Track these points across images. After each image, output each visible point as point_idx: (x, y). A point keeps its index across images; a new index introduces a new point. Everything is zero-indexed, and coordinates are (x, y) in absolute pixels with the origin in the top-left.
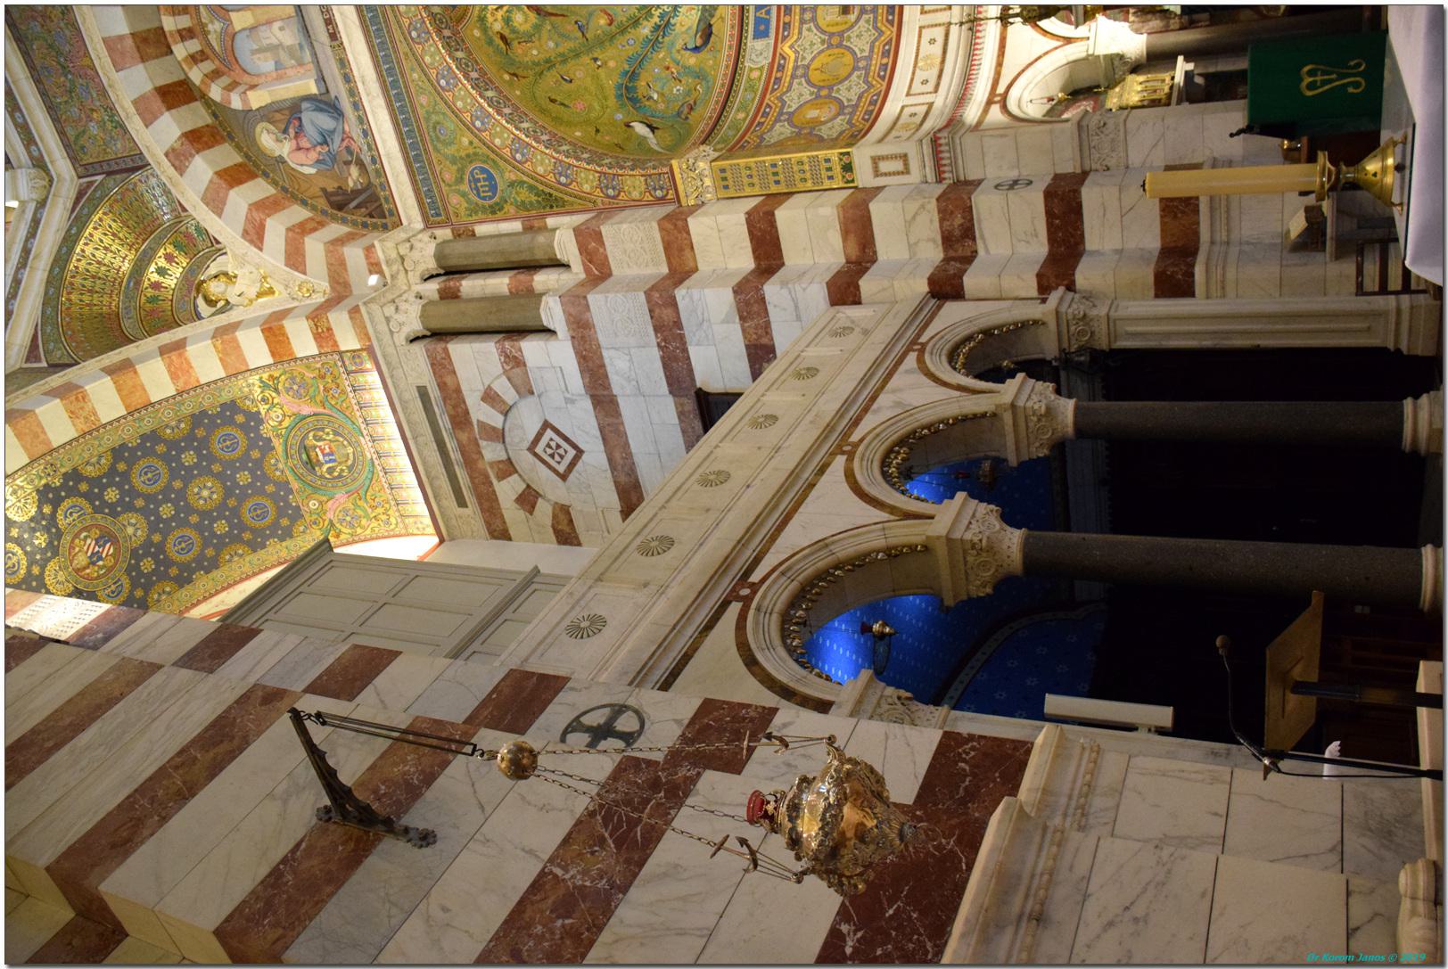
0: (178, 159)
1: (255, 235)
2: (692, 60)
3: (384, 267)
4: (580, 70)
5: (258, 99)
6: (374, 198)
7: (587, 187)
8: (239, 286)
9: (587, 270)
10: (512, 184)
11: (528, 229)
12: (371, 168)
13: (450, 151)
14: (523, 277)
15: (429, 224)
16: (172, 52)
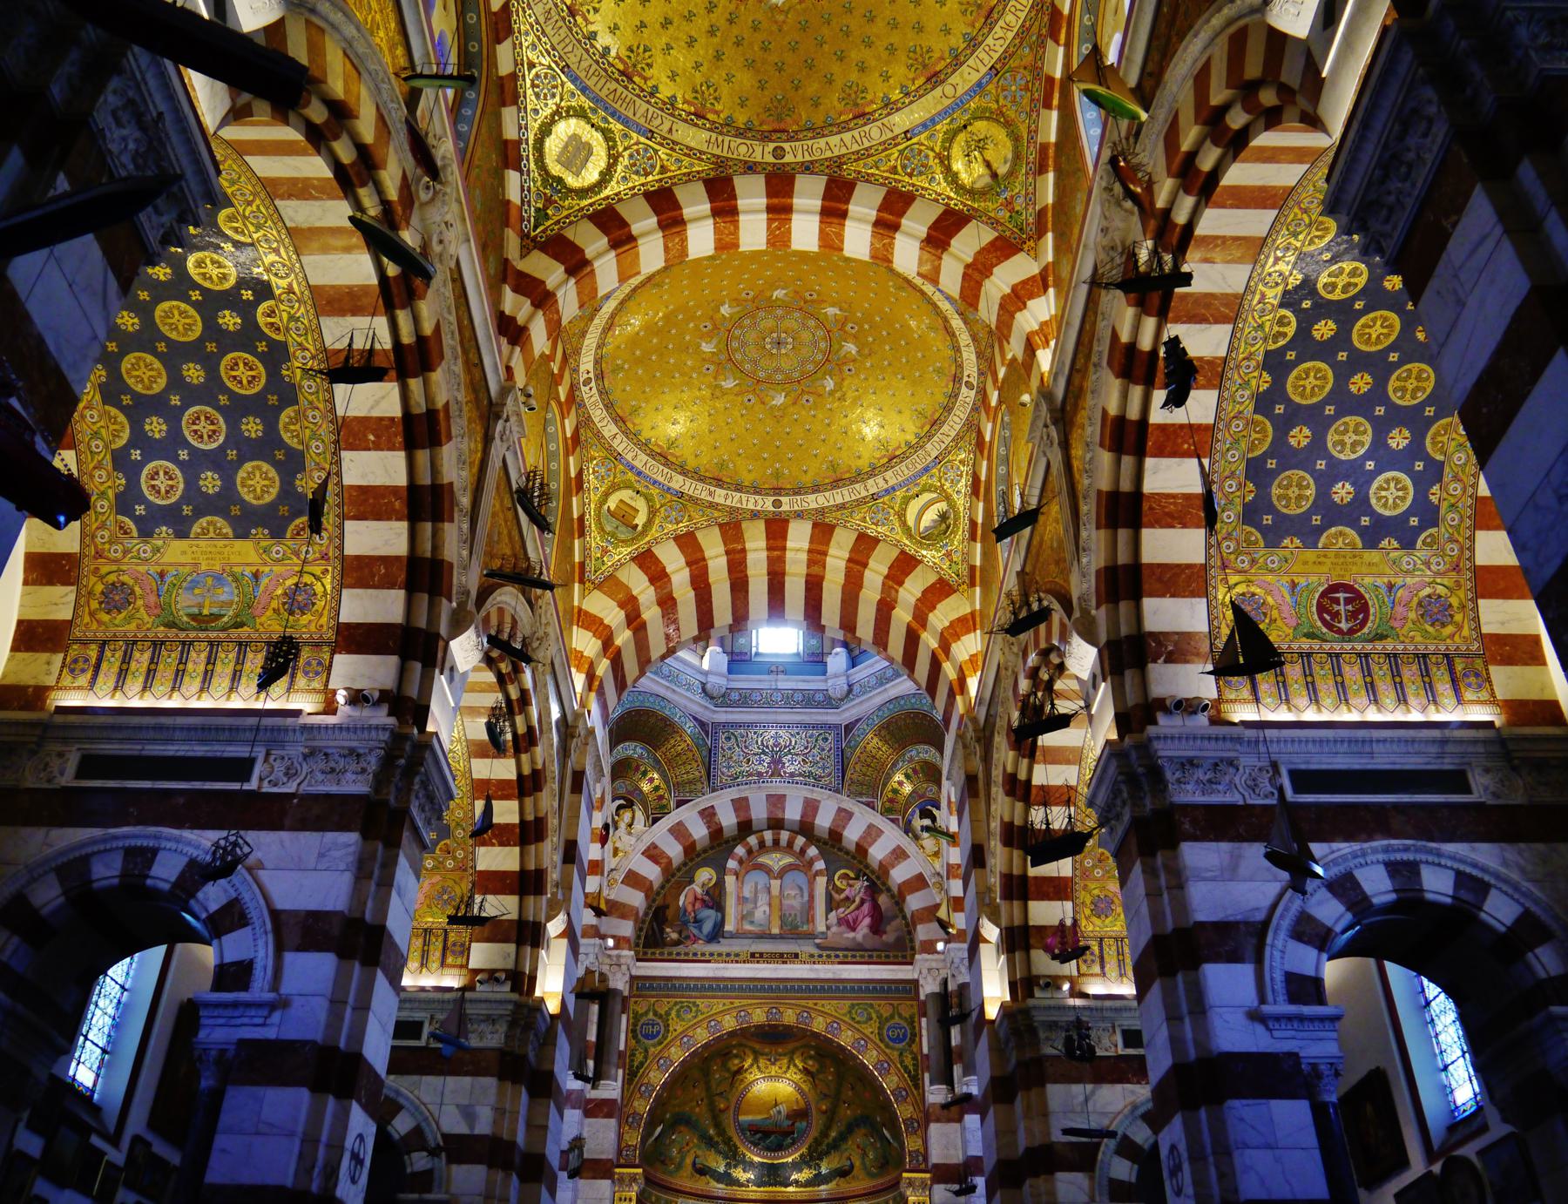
0: (708, 815)
1: (653, 853)
2: (689, 1161)
3: (615, 952)
4: (699, 1092)
5: (730, 880)
6: (656, 945)
7: (636, 1104)
8: (625, 838)
9: (591, 1101)
10: (646, 1051)
11: (621, 1055)
12: (675, 950)
13: (673, 1013)
14: (593, 1052)
15: (633, 978)
16: (769, 828)
